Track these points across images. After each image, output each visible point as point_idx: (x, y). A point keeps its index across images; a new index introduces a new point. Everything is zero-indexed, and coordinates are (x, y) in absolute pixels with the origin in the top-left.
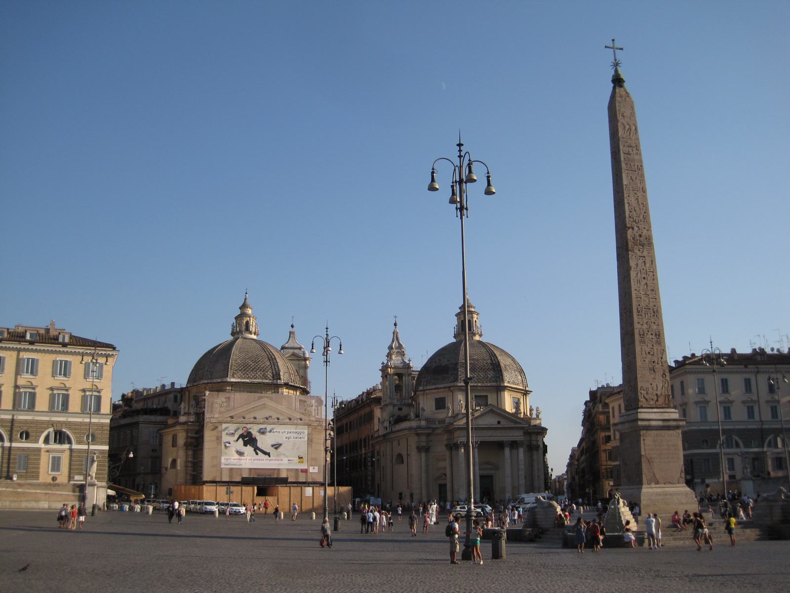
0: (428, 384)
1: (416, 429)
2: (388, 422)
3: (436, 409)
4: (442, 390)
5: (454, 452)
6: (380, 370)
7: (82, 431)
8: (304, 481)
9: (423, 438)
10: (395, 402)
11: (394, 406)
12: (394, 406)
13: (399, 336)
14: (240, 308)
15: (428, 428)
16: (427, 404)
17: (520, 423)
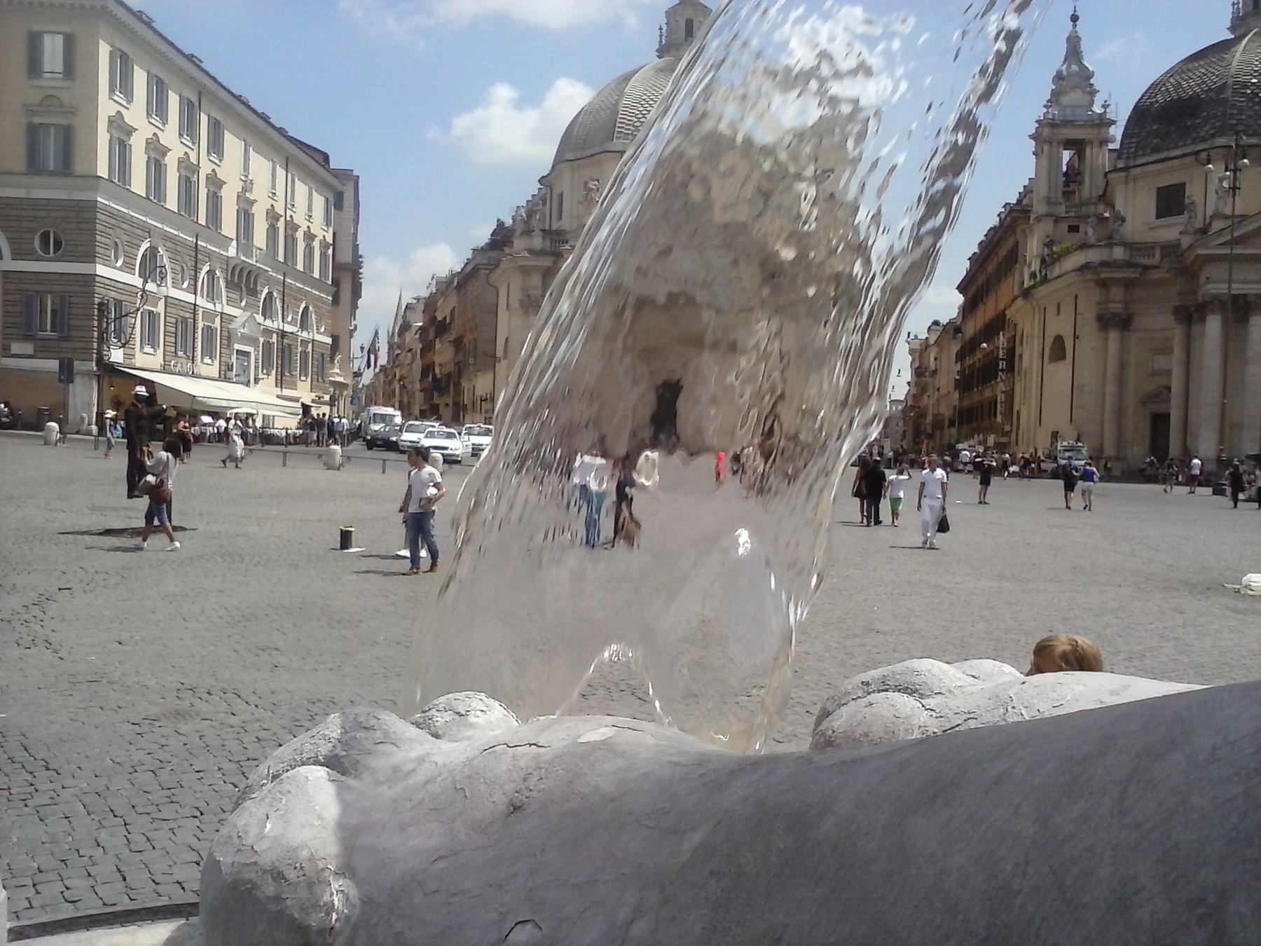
0: (1140, 153)
1: (1096, 268)
2: (1039, 261)
3: (1159, 215)
4: (1176, 162)
5: (1196, 329)
6: (1032, 137)
7: (25, 224)
9: (1117, 293)
10: (1061, 210)
11: (1057, 220)
12: (1057, 220)
13: (1085, 47)
15: (1128, 265)
16: (1136, 209)
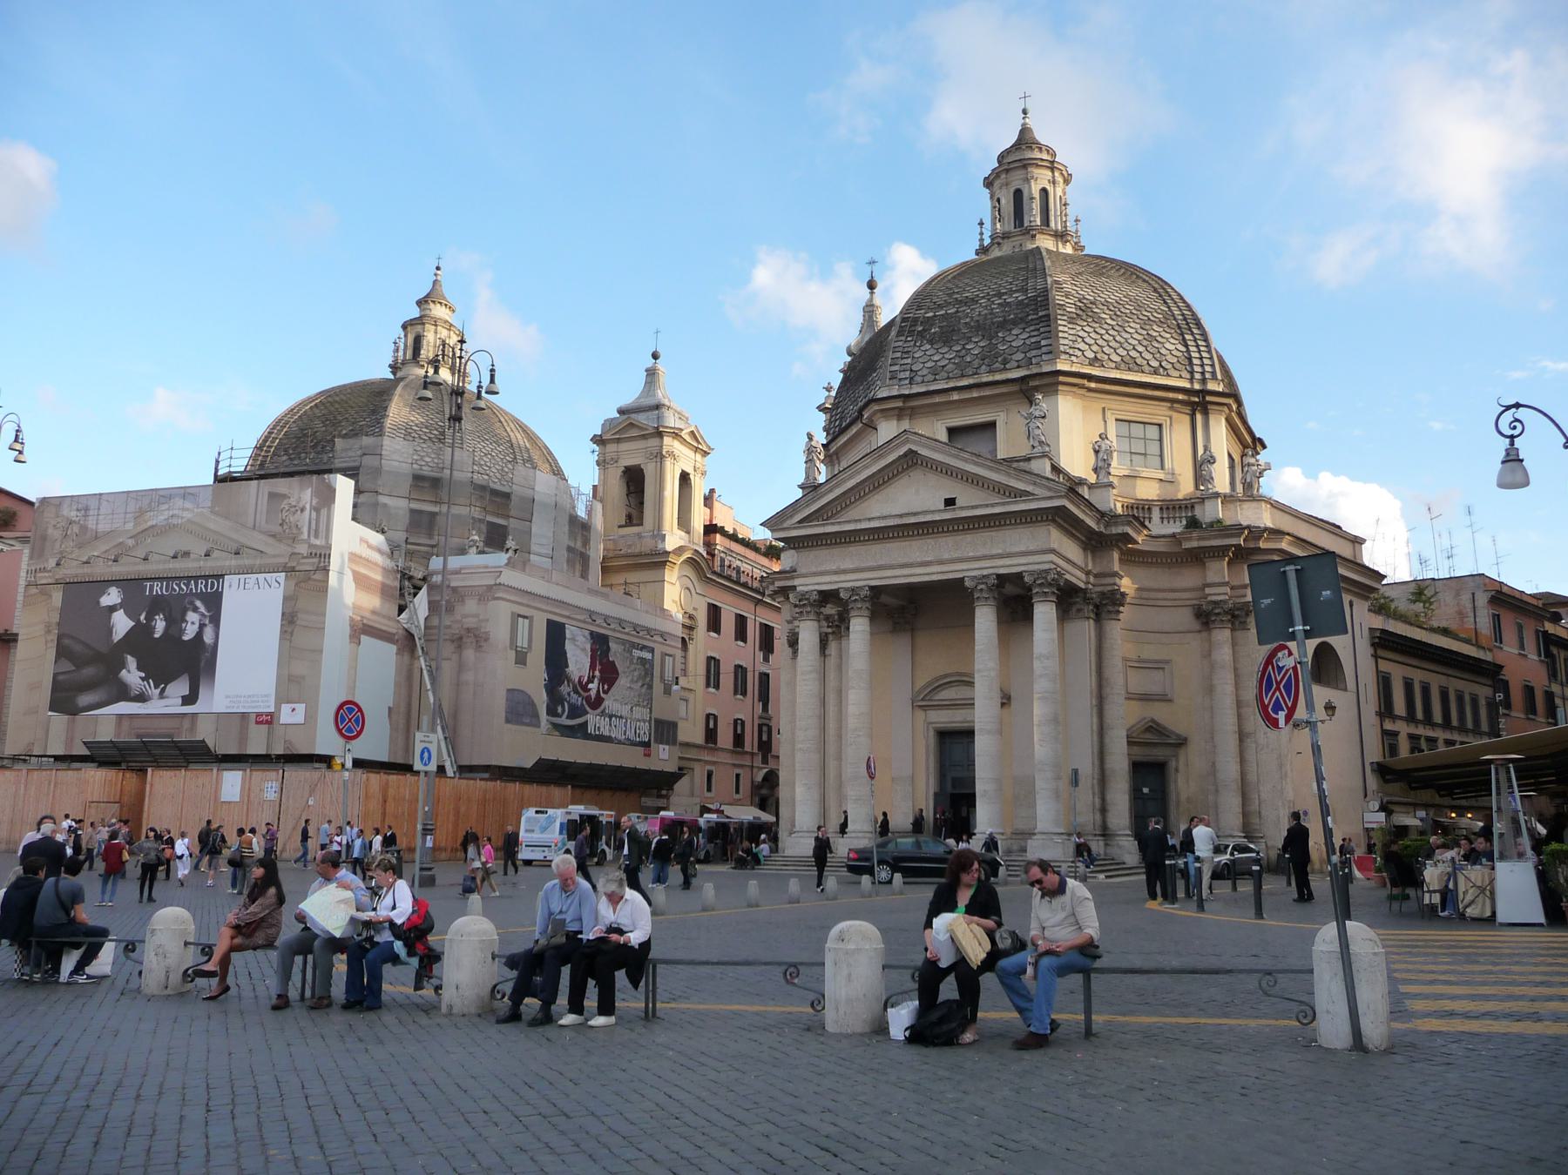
8: (263, 752)
14: (419, 303)
17: (1027, 493)
